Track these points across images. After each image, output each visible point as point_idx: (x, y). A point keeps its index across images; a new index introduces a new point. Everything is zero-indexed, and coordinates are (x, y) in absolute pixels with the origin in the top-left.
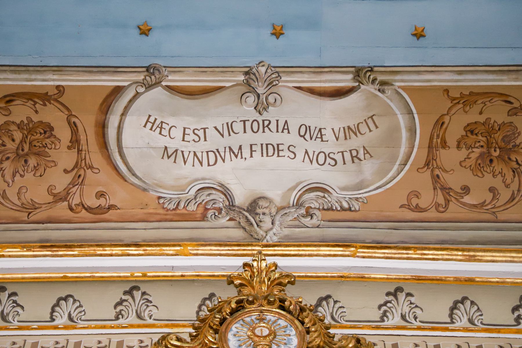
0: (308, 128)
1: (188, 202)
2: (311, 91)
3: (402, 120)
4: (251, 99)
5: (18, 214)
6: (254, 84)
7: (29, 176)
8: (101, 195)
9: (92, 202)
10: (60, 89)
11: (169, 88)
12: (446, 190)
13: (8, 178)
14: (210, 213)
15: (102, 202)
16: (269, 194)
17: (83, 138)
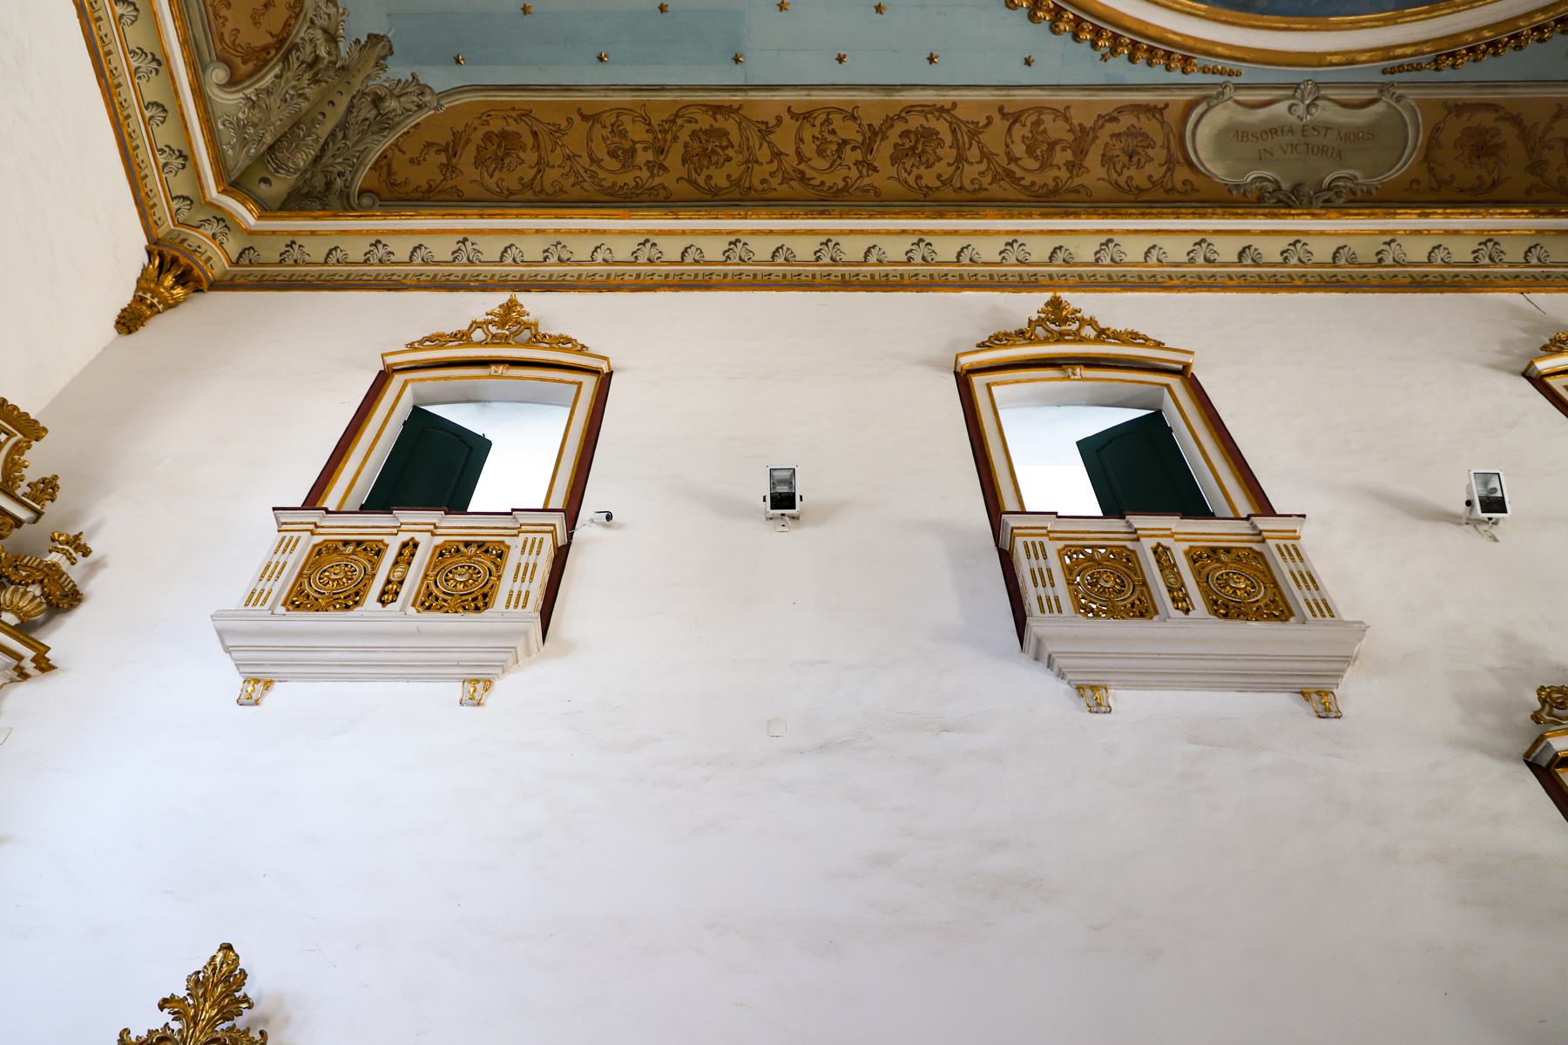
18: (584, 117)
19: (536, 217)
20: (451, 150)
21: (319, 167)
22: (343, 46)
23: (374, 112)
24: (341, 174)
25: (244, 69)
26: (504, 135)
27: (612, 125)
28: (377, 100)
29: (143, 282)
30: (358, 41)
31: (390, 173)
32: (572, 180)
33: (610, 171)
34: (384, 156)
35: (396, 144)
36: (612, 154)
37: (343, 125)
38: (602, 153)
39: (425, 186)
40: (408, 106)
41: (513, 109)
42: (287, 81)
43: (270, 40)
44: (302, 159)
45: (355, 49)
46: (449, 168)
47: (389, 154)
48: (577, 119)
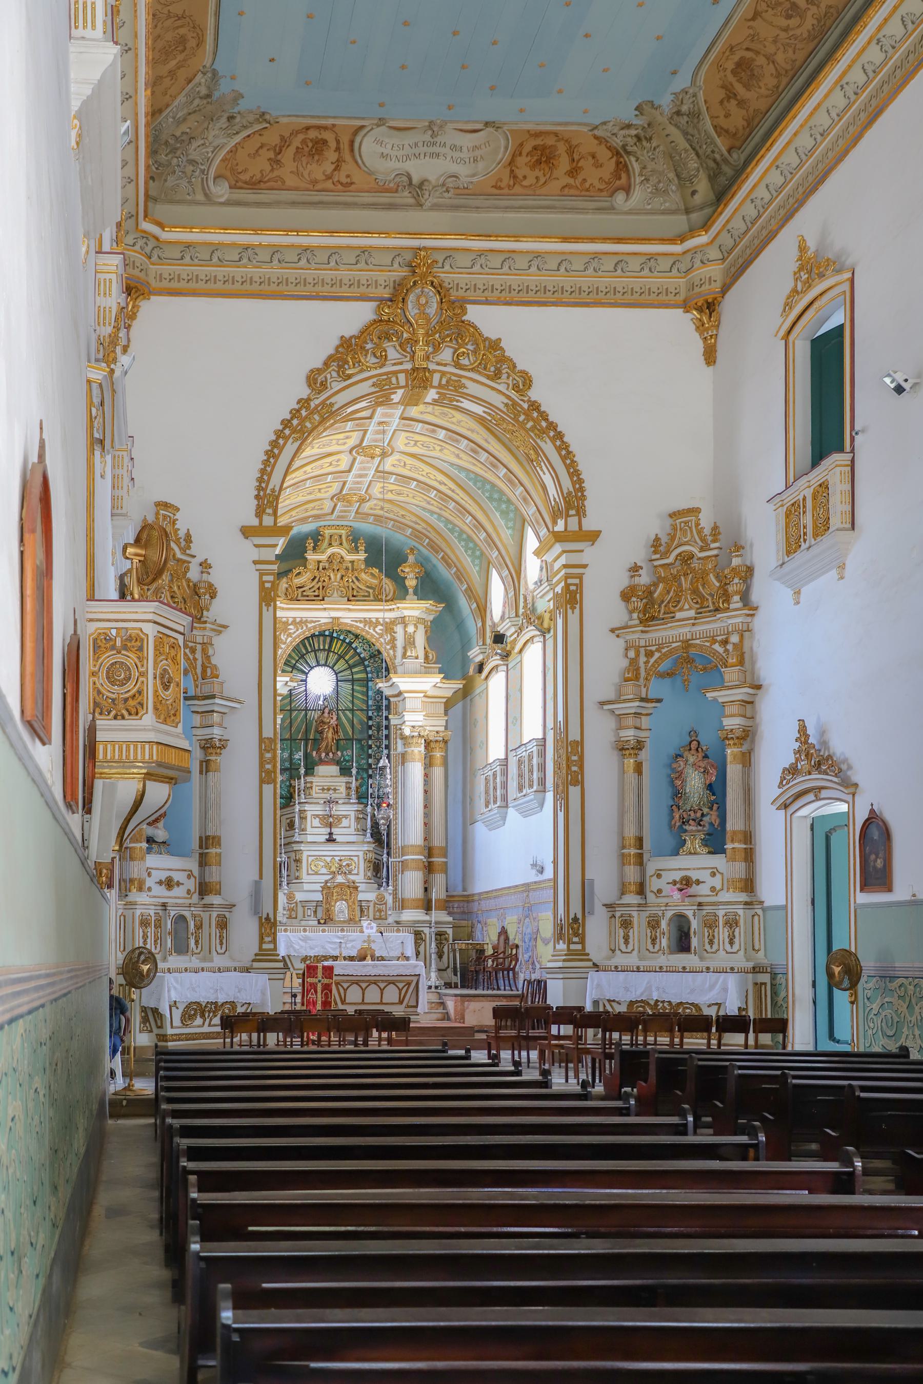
0: (455, 146)
1: (390, 182)
2: (461, 130)
3: (503, 143)
4: (430, 132)
5: (308, 186)
6: (433, 127)
7: (314, 165)
8: (348, 176)
9: (344, 180)
10: (334, 125)
11: (390, 127)
12: (515, 177)
13: (304, 165)
14: (400, 189)
15: (349, 180)
16: (430, 178)
17: (342, 146)
18: (753, 19)
19: (786, 127)
20: (731, 94)
21: (703, 157)
22: (635, 122)
23: (685, 117)
24: (713, 152)
25: (624, 180)
26: (739, 65)
27: (768, 6)
28: (678, 113)
29: (700, 327)
30: (636, 116)
31: (727, 131)
32: (791, 51)
33: (799, 26)
34: (715, 127)
35: (711, 117)
36: (788, 17)
37: (685, 134)
38: (784, 22)
39: (745, 124)
40: (691, 100)
41: (724, 53)
42: (643, 155)
43: (614, 159)
44: (693, 164)
45: (640, 117)
46: (741, 103)
47: (715, 123)
48: (751, 23)
